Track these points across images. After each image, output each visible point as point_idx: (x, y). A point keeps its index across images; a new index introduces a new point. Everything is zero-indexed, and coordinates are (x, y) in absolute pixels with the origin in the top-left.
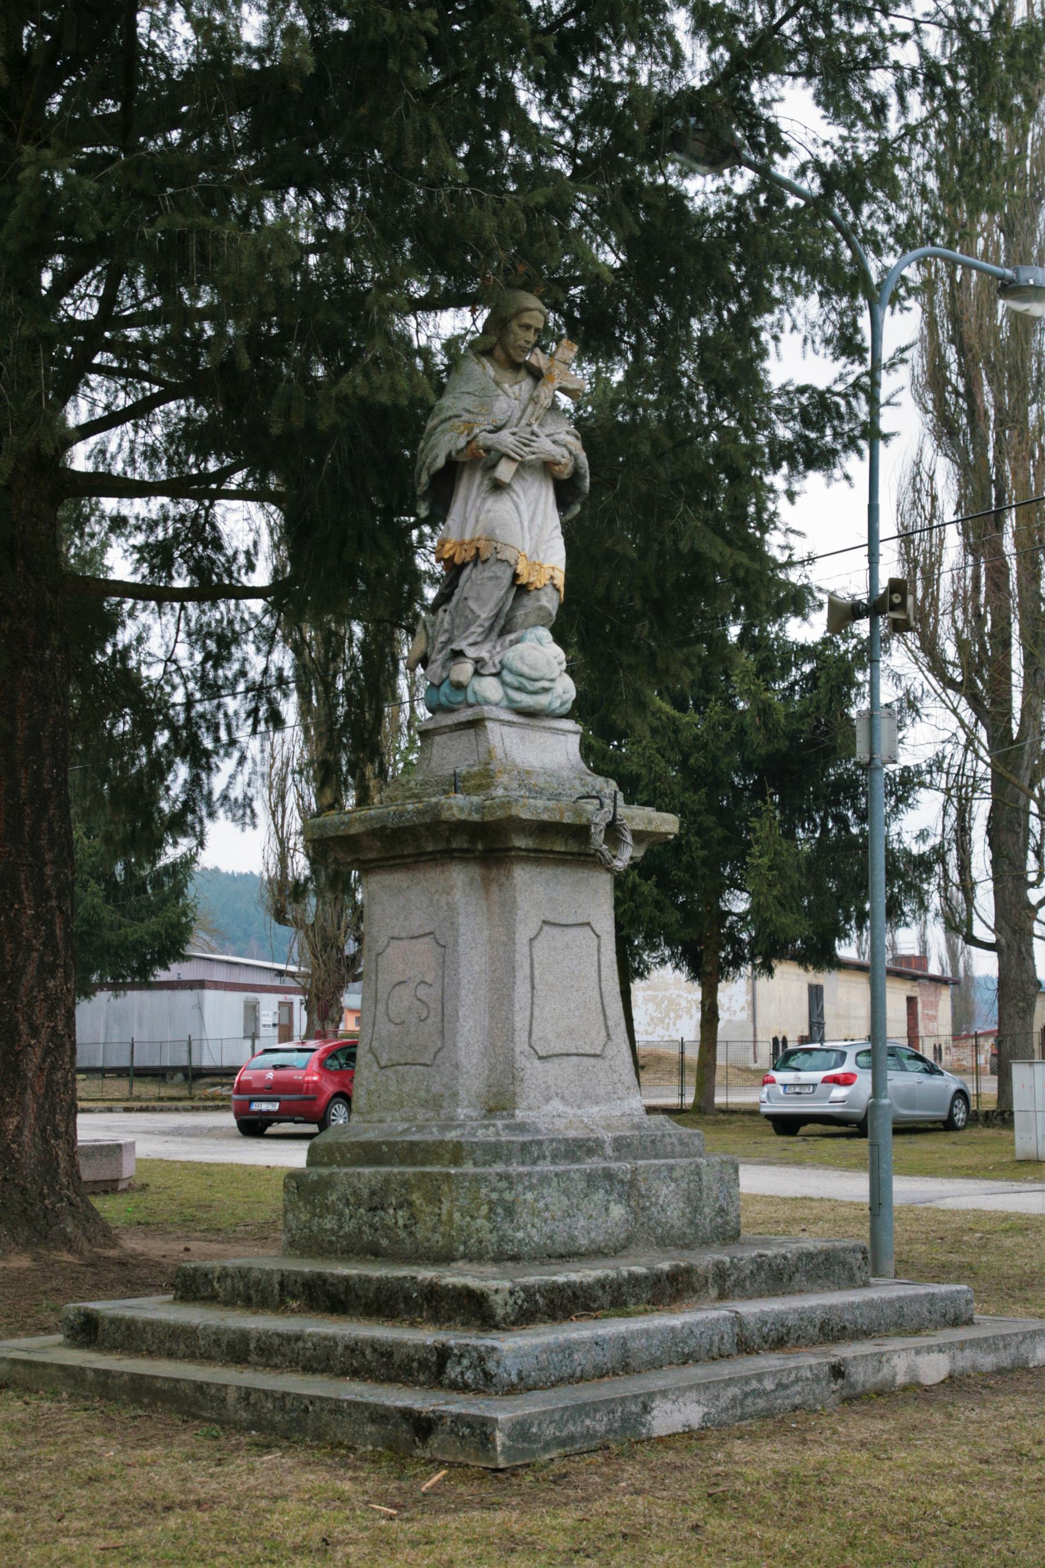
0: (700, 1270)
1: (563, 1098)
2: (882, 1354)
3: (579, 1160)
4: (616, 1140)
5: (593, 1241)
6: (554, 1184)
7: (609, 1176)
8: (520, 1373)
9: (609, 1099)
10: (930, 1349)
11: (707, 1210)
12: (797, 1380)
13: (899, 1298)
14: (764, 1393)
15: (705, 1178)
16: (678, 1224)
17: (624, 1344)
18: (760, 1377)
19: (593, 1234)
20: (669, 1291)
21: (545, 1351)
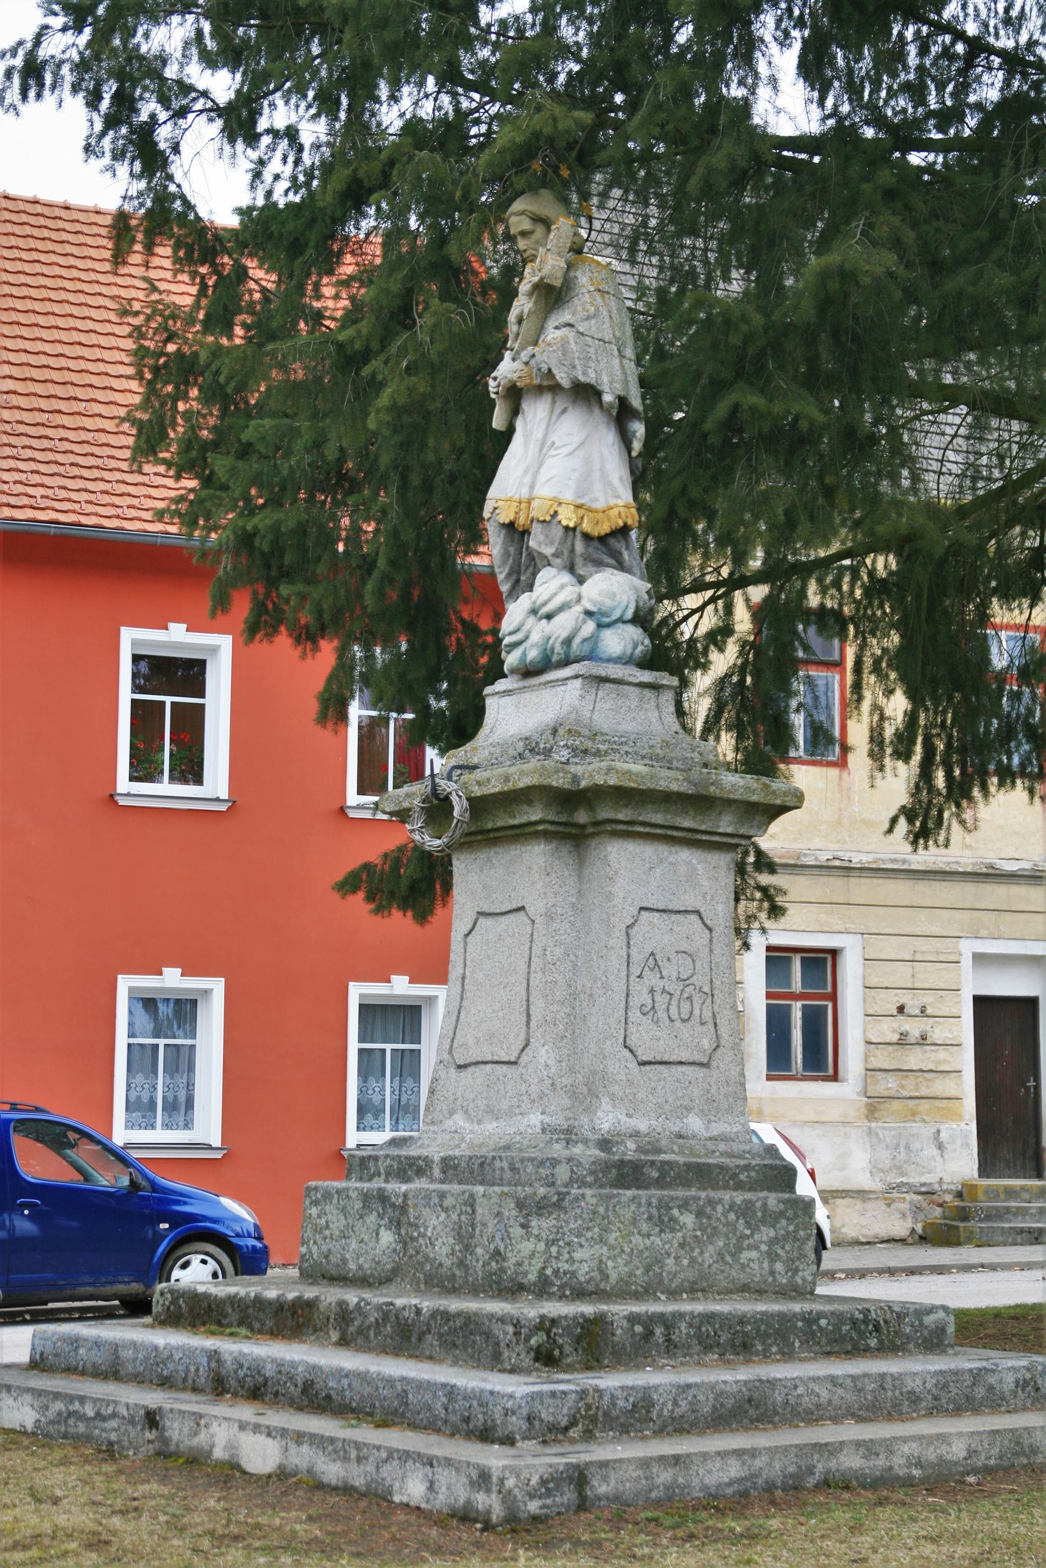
0: (322, 1307)
1: (466, 1112)
2: (201, 1416)
3: (407, 1180)
4: (444, 1160)
5: (360, 1267)
6: (335, 1201)
7: (382, 1197)
8: (42, 1353)
9: (510, 1113)
10: (257, 1428)
11: (479, 1251)
12: (114, 1415)
13: (403, 1379)
14: (81, 1417)
15: (479, 1210)
16: (448, 1263)
17: (116, 1350)
18: (82, 1399)
19: (361, 1260)
20: (290, 1322)
21: (59, 1339)
